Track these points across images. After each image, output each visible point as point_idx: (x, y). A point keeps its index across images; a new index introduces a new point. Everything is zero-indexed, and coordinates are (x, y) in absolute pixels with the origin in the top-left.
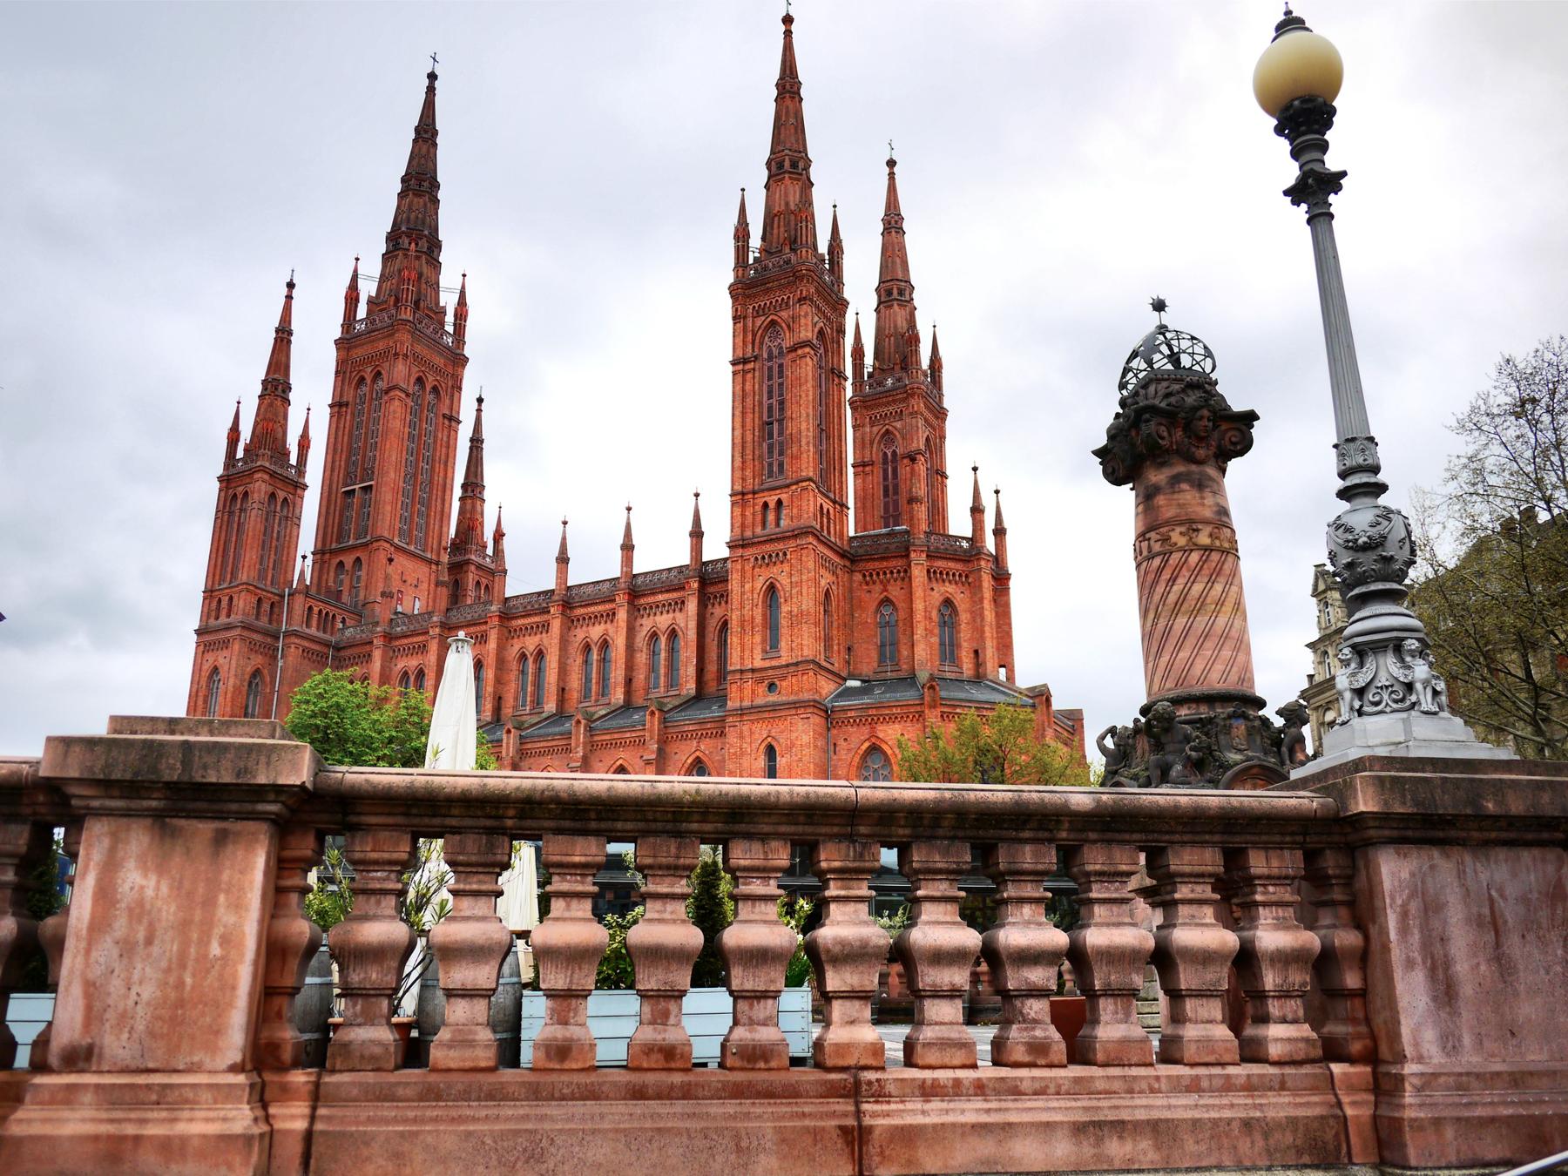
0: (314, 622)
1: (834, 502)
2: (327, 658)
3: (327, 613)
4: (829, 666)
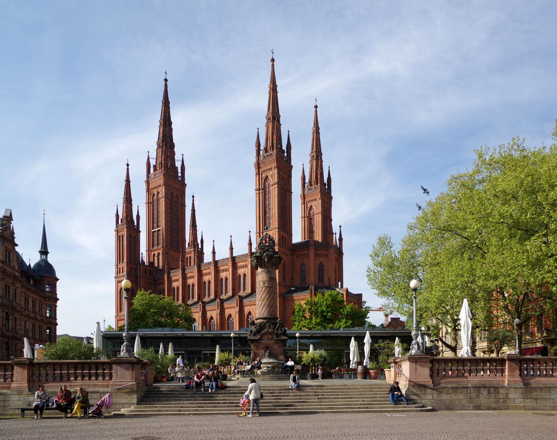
0: (147, 273)
1: (287, 234)
2: (152, 283)
3: (151, 270)
4: (285, 284)
